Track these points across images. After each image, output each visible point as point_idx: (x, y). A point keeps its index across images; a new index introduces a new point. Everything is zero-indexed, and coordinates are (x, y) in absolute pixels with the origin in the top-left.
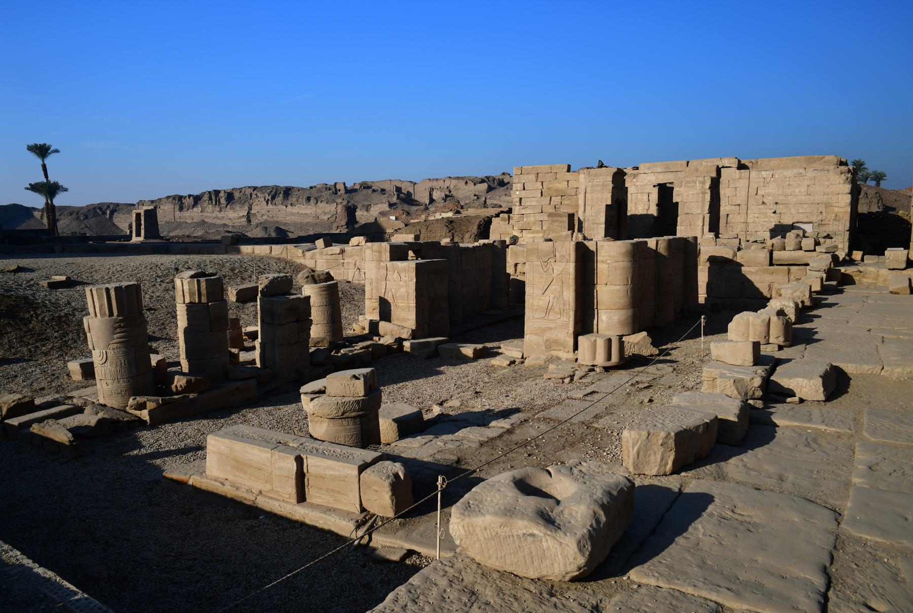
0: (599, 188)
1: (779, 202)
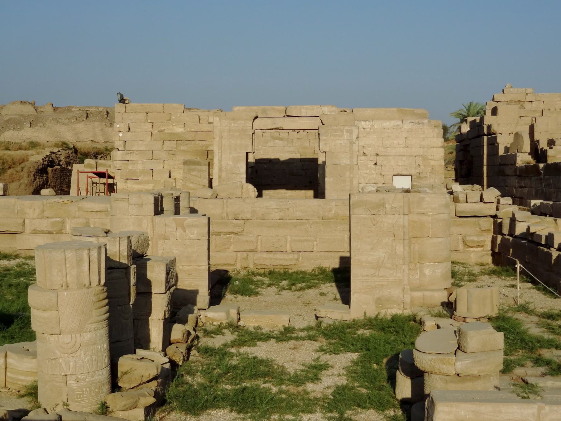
1: (379, 154)
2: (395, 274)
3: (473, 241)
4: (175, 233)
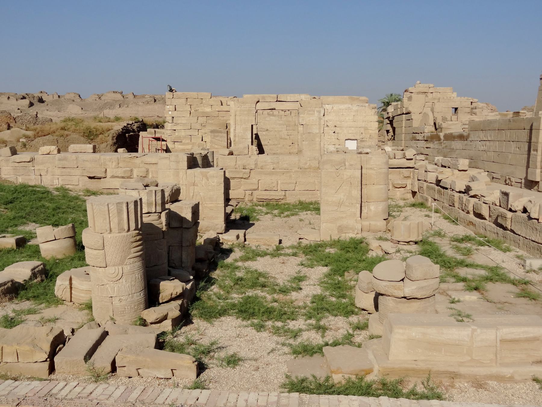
0: (246, 113)
2: (351, 210)
3: (399, 184)
4: (201, 181)
